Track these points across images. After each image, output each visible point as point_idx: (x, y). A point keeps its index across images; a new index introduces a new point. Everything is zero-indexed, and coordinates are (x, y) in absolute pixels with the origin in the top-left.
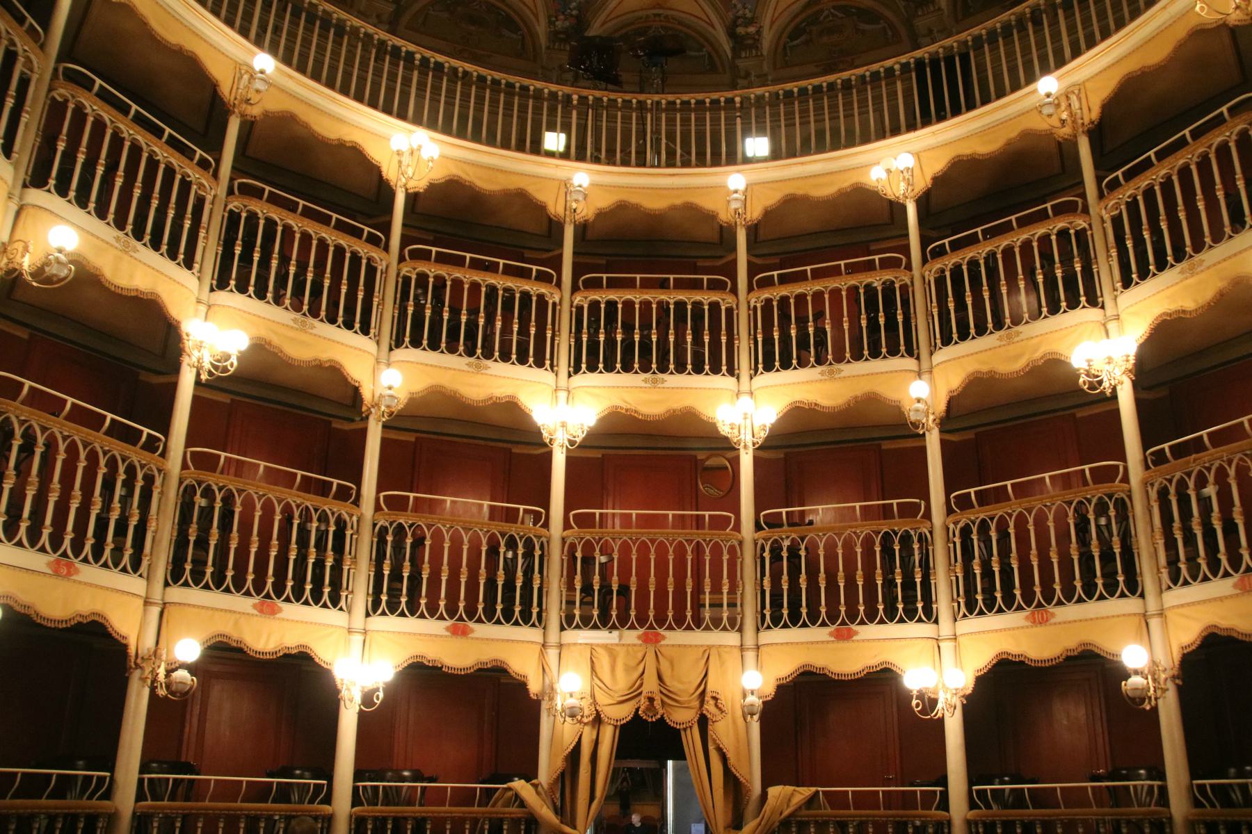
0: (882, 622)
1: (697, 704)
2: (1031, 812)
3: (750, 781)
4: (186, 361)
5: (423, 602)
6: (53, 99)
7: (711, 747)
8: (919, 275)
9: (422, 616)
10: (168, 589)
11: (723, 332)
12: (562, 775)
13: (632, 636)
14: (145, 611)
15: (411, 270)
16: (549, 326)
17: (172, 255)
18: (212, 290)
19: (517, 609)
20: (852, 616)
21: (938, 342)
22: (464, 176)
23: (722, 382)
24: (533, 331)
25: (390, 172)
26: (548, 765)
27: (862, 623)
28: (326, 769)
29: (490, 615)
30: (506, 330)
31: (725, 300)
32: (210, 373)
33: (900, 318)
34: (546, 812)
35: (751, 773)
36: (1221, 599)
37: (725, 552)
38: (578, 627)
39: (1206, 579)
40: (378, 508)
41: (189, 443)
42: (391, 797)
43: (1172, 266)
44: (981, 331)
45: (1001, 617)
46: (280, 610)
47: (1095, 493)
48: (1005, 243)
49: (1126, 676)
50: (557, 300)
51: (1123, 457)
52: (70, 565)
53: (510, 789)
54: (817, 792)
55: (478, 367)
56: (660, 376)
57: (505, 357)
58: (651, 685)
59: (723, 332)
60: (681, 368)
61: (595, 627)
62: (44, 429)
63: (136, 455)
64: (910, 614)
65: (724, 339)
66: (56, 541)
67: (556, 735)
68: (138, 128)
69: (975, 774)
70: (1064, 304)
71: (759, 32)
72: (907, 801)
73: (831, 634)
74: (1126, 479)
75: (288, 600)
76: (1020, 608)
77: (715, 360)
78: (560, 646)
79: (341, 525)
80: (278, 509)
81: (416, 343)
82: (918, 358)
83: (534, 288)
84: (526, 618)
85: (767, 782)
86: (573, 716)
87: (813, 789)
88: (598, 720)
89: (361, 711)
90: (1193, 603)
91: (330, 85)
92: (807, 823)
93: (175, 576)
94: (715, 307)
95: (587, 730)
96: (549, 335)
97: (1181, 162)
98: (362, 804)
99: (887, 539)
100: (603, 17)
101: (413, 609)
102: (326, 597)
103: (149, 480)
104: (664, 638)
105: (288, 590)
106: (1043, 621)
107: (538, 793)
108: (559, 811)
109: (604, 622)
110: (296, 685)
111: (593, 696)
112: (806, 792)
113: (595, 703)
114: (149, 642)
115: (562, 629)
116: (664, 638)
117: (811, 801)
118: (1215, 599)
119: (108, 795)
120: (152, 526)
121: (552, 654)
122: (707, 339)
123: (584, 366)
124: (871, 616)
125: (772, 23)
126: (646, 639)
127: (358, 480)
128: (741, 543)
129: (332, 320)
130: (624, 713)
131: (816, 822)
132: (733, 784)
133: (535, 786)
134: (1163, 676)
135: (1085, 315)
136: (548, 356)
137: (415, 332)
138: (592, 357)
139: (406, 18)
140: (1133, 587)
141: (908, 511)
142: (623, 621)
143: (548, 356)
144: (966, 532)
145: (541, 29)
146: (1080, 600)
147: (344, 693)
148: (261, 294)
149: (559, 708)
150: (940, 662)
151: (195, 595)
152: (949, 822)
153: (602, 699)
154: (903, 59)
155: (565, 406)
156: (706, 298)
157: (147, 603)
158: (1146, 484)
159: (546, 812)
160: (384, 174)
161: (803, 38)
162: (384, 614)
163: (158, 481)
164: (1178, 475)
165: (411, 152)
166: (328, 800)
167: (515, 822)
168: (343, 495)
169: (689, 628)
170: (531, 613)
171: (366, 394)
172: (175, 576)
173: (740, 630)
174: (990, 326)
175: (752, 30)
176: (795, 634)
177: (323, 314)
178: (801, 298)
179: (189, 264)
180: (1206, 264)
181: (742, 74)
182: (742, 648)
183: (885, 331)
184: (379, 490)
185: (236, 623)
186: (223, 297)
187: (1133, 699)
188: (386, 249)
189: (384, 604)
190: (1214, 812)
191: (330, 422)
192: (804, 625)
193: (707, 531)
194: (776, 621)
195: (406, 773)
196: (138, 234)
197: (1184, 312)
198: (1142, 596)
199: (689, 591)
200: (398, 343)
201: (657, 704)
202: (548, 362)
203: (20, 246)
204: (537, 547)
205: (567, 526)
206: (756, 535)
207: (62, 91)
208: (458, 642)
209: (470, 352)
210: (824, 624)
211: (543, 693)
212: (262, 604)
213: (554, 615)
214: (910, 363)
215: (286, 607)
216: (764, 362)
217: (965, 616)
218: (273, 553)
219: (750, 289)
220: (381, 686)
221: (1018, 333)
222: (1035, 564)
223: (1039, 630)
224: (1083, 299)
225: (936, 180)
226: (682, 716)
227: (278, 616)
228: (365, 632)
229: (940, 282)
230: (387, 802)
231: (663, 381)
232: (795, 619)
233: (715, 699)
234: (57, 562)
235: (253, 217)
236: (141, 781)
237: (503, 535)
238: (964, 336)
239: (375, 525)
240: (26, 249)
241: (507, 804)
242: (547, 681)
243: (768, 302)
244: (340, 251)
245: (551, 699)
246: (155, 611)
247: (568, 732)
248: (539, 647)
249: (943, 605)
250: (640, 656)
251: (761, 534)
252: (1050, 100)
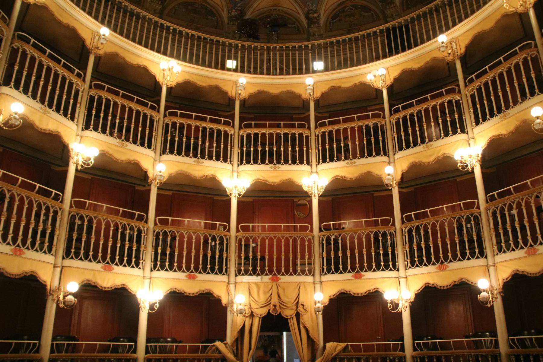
0: (374, 271)
1: (295, 307)
2: (440, 352)
3: (319, 341)
4: (71, 161)
5: (176, 264)
6: (13, 47)
7: (301, 326)
8: (389, 121)
9: (175, 271)
10: (64, 260)
11: (305, 146)
12: (237, 339)
13: (266, 278)
14: (54, 270)
15: (169, 120)
16: (229, 144)
17: (65, 115)
18: (83, 130)
19: (217, 267)
20: (362, 268)
21: (397, 149)
22: (192, 80)
23: (304, 168)
24: (222, 146)
25: (160, 78)
26: (231, 335)
27: (366, 271)
28: (134, 338)
29: (205, 270)
30: (211, 146)
31: (305, 132)
32: (82, 166)
33: (380, 139)
34: (230, 356)
35: (319, 337)
36: (520, 258)
37: (306, 241)
38: (243, 275)
39: (513, 250)
40: (155, 224)
41: (73, 197)
42: (163, 350)
43: (497, 115)
44: (415, 144)
45: (425, 268)
46: (113, 269)
47: (466, 213)
48: (425, 106)
49: (480, 292)
50: (232, 133)
51: (477, 198)
52: (21, 250)
53: (214, 346)
54: (348, 345)
55: (199, 162)
56: (278, 165)
57: (210, 158)
58: (275, 300)
59: (305, 146)
60: (286, 162)
61: (250, 275)
62: (9, 191)
63: (50, 202)
64: (387, 267)
65: (305, 149)
66: (15, 240)
67: (234, 321)
68: (50, 60)
69: (416, 336)
70: (451, 132)
71: (319, 16)
72: (386, 348)
73: (352, 276)
74: (478, 207)
75: (116, 264)
76: (434, 264)
77: (301, 158)
78: (235, 283)
79: (140, 232)
80: (112, 225)
81: (172, 152)
82: (389, 156)
83: (223, 128)
84: (220, 271)
85: (326, 341)
86: (241, 313)
87: (346, 344)
88: (252, 315)
89: (149, 312)
90: (508, 261)
91: (134, 40)
92: (343, 359)
93: (67, 254)
94: (301, 135)
95: (247, 319)
96: (229, 148)
97: (500, 71)
98: (150, 353)
99: (376, 235)
100: (251, 10)
101: (171, 268)
102: (133, 263)
103: (56, 213)
104: (280, 279)
105: (117, 260)
106: (444, 269)
107: (226, 347)
108: (236, 355)
109: (254, 272)
110: (121, 301)
111: (250, 304)
112: (343, 345)
113: (251, 308)
114: (56, 284)
115: (236, 275)
116: (280, 279)
117: (345, 349)
118: (517, 259)
120: (57, 233)
121: (232, 286)
122: (297, 149)
123: (244, 162)
124: (370, 268)
125: (324, 13)
126: (272, 280)
127: (147, 212)
128: (313, 237)
129: (135, 142)
130: (263, 312)
131: (347, 358)
132: (311, 342)
133: (225, 344)
134: (496, 292)
135: (460, 137)
136: (229, 157)
137: (171, 147)
138: (248, 157)
139: (167, 11)
140: (482, 254)
141: (385, 223)
142: (263, 272)
143: (229, 157)
144: (410, 231)
145: (225, 16)
146: (460, 260)
147: (141, 305)
148: (104, 132)
149: (235, 310)
150: (399, 288)
151: (76, 263)
152: (405, 357)
153: (254, 306)
154: (381, 28)
155: (236, 179)
156: (297, 131)
157: (55, 266)
158: (487, 209)
159: (230, 356)
160: (157, 79)
161: (338, 19)
162: (158, 270)
163: (59, 213)
164: (500, 205)
165: (168, 69)
166: (135, 351)
167: (217, 360)
168: (140, 218)
169: (291, 275)
170: (222, 269)
171: (150, 174)
172: (67, 254)
173: (313, 275)
174: (419, 142)
175: (316, 15)
176: (337, 277)
177: (131, 140)
178: (338, 131)
179: (72, 118)
180: (510, 115)
181: (312, 34)
182: (314, 283)
183: (374, 146)
184: (156, 216)
185: (94, 275)
186: (87, 133)
187: (482, 302)
188: (158, 111)
189: (158, 266)
190: (519, 350)
191: (135, 187)
192: (341, 273)
193: (298, 232)
194: (329, 271)
195: (169, 339)
196: (50, 106)
197: (502, 135)
198: (486, 257)
199: (291, 258)
200: (164, 152)
201: (278, 308)
202: (229, 160)
204: (225, 240)
205: (238, 231)
206: (320, 234)
207: (17, 44)
208: (191, 282)
209: (195, 156)
210: (349, 272)
211: (228, 303)
212: (105, 266)
213: (233, 270)
214: (385, 159)
215: (116, 267)
216: (322, 159)
217: (410, 267)
218: (110, 244)
219: (316, 127)
220: (158, 301)
221: (431, 145)
222: (440, 244)
223: (442, 273)
224: (459, 130)
225: (396, 79)
226: (288, 313)
227: (112, 271)
228: (150, 278)
229: (398, 123)
230: (161, 352)
231: (279, 168)
232: (337, 270)
233: (303, 305)
234: (15, 249)
235: (100, 98)
236: (52, 345)
237: (210, 235)
238: (408, 147)
239: (154, 231)
241: (213, 352)
242: (230, 299)
243: (324, 133)
244: (138, 112)
245: (232, 306)
246: (58, 270)
247: (239, 320)
248: (226, 284)
249: (401, 263)
250: (270, 287)
251: (322, 233)
252: (443, 45)
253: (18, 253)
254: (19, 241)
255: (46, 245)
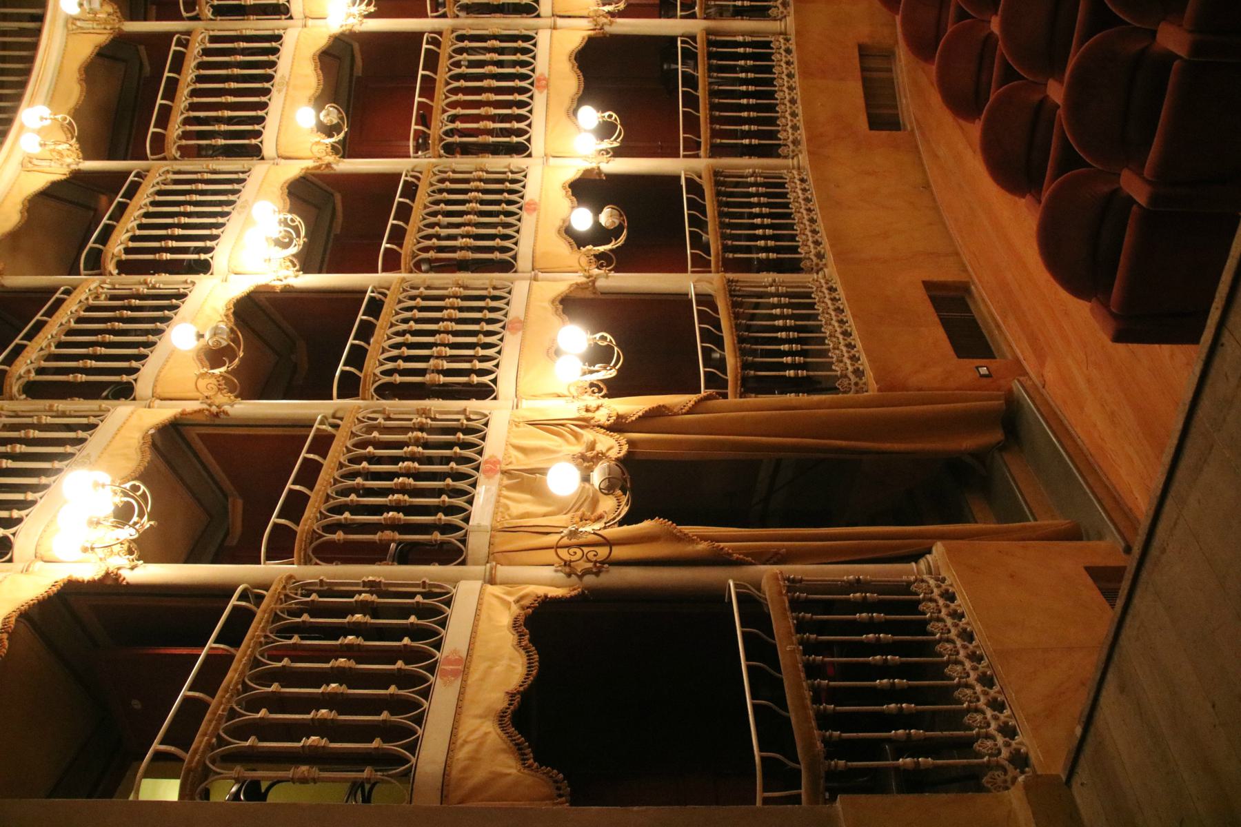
4: (358, 28)
10: (542, 14)
17: (275, 51)
18: (291, 18)
32: (368, 4)
52: (539, 80)
66: (523, 91)
103: (461, 38)
119: (694, 38)
157: (554, 28)
163: (460, 32)
196: (270, 78)
203: (315, 149)
236: (682, 17)
240: (318, 143)
246: (560, 21)
253: (544, 83)
254: (524, 84)
255: (520, 44)
